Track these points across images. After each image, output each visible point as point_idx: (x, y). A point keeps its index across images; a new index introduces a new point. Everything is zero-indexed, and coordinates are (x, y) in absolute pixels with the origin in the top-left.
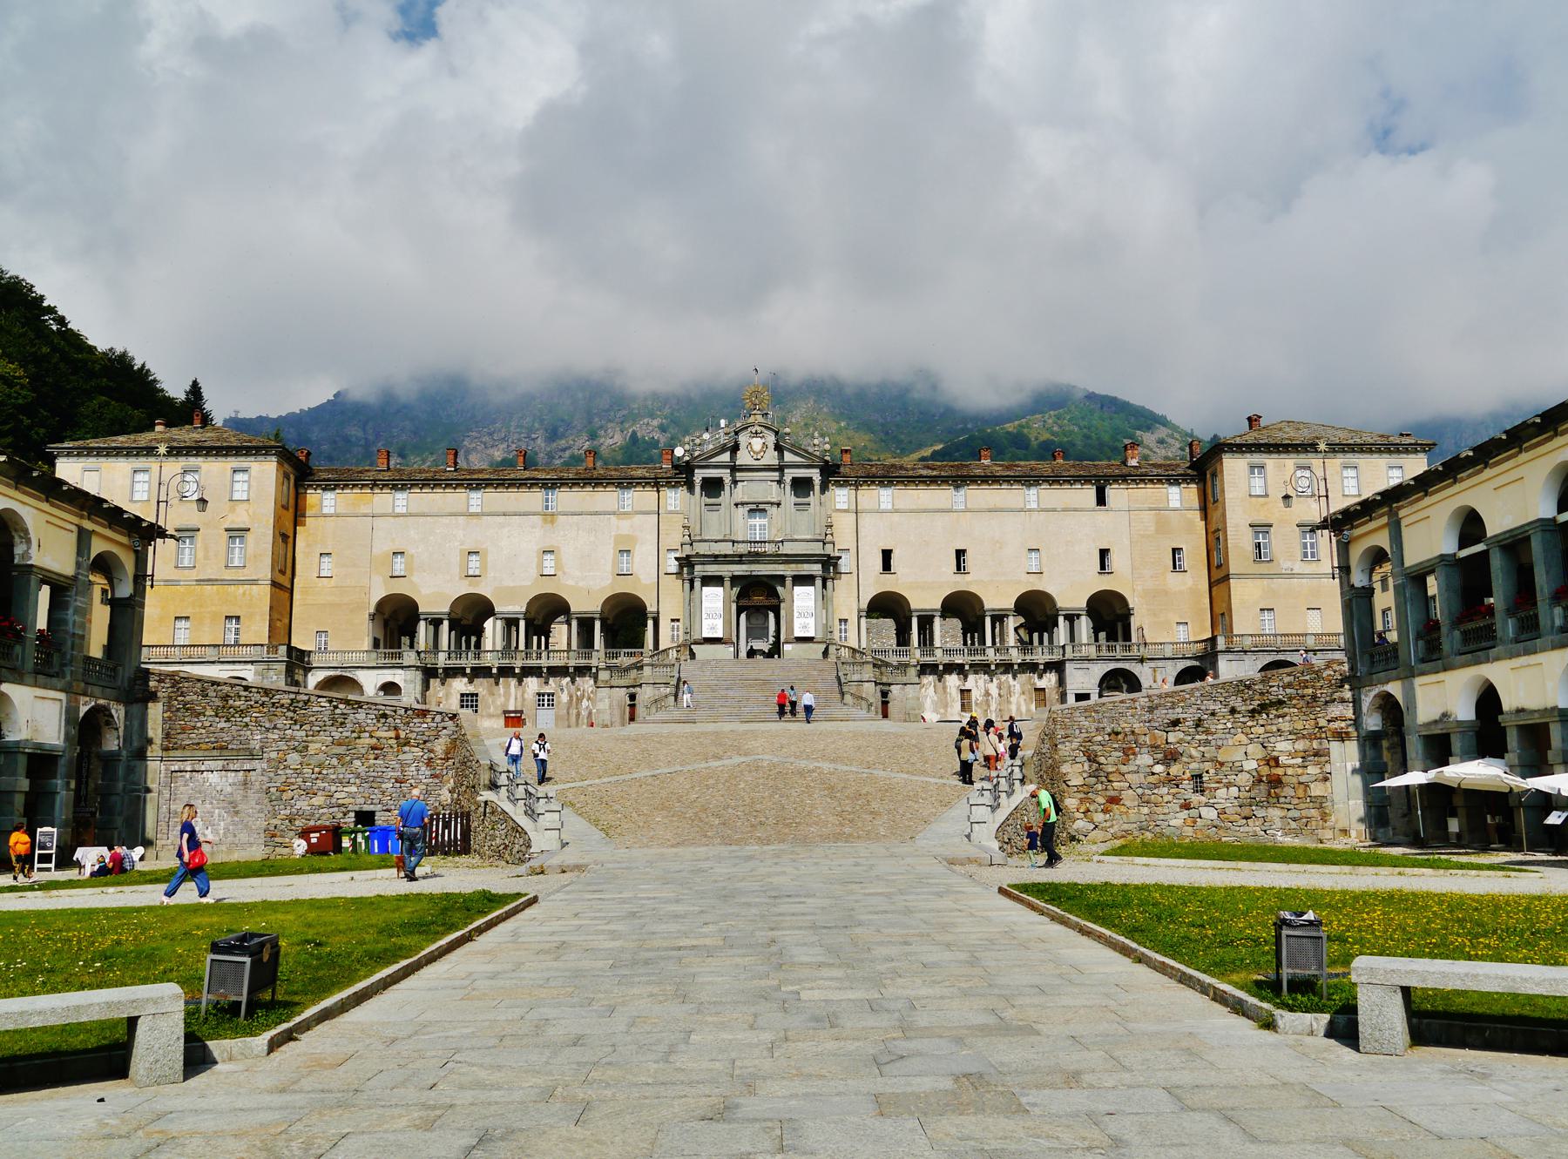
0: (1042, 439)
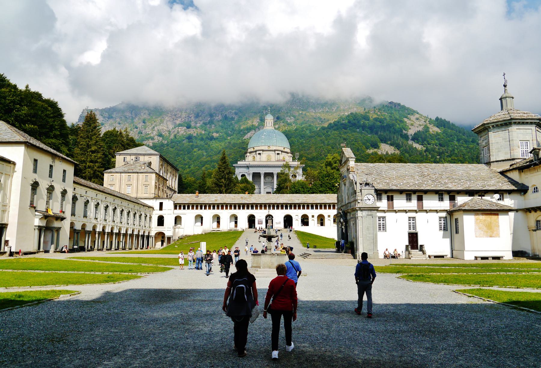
0: (374, 117)
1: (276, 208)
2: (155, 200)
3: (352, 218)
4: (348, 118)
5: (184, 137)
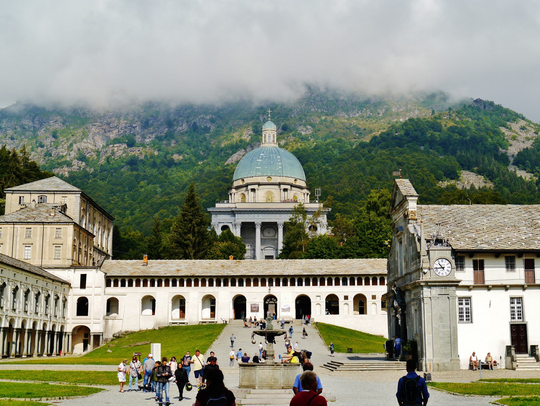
1: (281, 283)
2: (73, 270)
3: (413, 300)
4: (404, 127)
5: (123, 162)
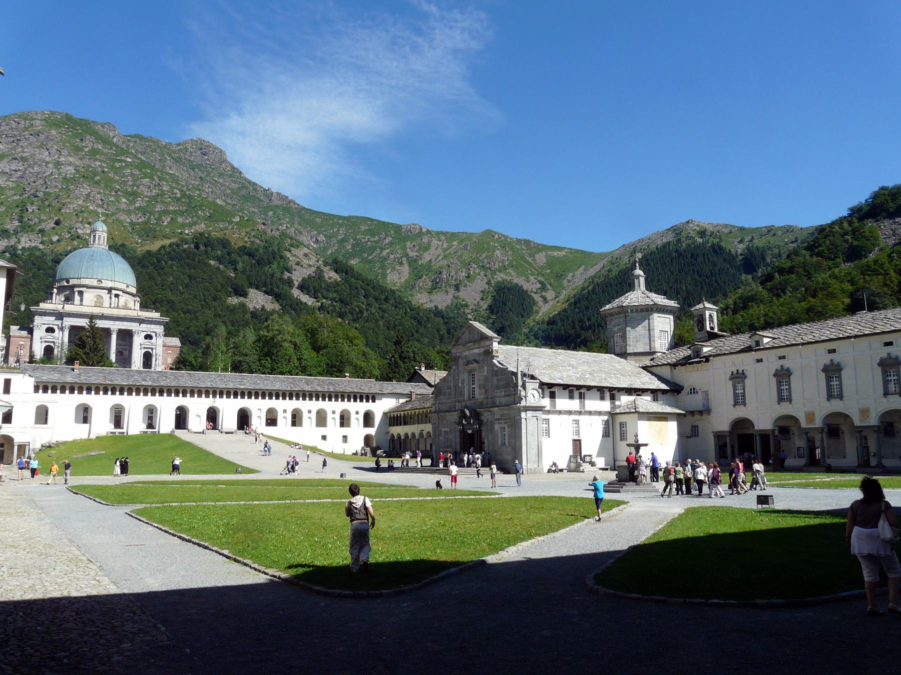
3: (498, 419)
